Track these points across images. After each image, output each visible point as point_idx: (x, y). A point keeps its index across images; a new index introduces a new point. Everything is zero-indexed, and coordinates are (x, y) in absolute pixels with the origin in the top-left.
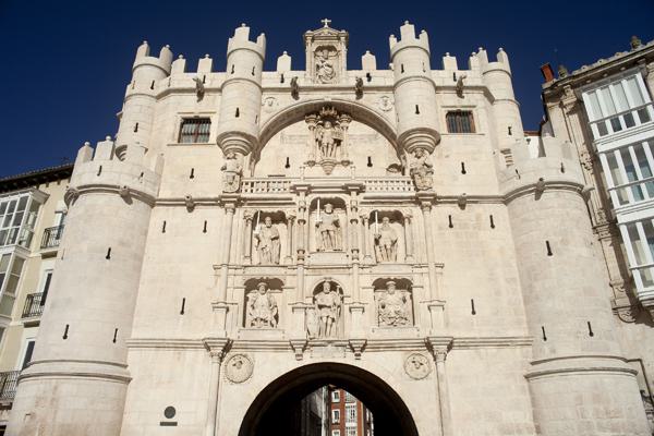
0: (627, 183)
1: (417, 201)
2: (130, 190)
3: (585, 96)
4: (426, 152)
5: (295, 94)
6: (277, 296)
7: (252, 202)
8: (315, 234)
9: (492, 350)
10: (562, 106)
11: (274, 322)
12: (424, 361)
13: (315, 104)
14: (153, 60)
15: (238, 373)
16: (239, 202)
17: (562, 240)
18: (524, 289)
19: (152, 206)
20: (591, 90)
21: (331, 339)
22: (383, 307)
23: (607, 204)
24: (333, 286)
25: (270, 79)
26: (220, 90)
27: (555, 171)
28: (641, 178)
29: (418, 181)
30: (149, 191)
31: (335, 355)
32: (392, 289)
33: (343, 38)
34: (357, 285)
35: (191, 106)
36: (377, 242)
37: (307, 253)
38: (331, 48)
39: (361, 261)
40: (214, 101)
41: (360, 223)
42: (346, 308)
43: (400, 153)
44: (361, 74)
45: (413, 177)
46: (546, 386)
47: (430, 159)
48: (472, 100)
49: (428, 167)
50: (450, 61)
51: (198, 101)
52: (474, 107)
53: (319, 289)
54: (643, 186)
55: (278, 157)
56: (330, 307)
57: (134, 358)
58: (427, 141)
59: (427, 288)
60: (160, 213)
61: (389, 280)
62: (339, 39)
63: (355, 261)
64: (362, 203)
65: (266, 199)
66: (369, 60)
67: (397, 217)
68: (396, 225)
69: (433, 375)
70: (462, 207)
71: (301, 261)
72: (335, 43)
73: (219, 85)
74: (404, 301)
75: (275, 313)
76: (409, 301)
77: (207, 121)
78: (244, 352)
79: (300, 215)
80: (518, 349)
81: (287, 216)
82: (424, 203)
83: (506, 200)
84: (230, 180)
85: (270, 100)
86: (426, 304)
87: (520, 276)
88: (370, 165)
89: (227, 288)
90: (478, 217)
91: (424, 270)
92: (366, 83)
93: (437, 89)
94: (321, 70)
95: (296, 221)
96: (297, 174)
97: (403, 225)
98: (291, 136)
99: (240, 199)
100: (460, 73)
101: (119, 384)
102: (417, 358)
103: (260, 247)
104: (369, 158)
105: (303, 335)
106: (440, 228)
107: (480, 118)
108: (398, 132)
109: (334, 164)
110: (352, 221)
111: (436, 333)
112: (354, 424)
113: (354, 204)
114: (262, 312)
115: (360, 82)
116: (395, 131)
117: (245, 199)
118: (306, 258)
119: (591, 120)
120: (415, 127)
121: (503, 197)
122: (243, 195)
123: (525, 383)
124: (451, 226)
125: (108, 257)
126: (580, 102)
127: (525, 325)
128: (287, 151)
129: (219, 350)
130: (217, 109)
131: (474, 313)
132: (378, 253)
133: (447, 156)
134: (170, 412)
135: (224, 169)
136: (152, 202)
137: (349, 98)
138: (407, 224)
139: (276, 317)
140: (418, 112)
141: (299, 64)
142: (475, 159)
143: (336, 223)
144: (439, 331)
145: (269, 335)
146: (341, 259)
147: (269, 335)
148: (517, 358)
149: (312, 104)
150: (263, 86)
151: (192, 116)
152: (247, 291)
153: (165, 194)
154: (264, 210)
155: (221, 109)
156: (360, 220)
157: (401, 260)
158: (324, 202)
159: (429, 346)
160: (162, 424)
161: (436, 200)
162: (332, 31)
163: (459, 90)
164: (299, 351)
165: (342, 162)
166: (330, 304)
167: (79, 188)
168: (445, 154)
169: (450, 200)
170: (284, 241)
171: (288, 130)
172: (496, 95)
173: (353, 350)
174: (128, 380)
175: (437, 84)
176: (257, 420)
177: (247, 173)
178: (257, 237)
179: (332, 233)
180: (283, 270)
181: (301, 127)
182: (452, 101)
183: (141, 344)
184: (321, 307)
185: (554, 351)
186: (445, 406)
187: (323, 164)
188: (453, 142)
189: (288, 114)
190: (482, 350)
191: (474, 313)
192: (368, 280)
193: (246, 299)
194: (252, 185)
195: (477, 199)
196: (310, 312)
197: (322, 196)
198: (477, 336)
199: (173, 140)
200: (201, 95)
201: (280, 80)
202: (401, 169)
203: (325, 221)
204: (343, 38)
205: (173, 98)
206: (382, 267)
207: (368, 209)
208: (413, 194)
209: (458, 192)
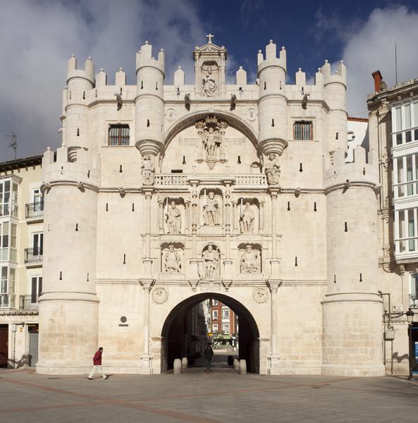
0: (406, 182)
1: (268, 191)
2: (84, 184)
3: (394, 110)
5: (188, 107)
6: (180, 252)
7: (163, 191)
8: (202, 213)
9: (305, 288)
10: (378, 115)
11: (179, 269)
12: (264, 292)
13: (202, 114)
14: (80, 73)
16: (154, 191)
18: (328, 252)
19: (98, 192)
20: (398, 106)
23: (391, 194)
24: (214, 247)
25: (169, 93)
26: (134, 102)
28: (414, 179)
29: (270, 178)
30: (95, 184)
33: (222, 54)
34: (229, 247)
35: (112, 114)
36: (241, 219)
37: (198, 227)
38: (213, 63)
39: (231, 232)
42: (222, 261)
43: (259, 154)
45: (267, 174)
46: (331, 308)
47: (279, 160)
48: (313, 111)
49: (278, 168)
50: (300, 76)
51: (118, 110)
53: (206, 248)
54: (415, 184)
57: (99, 289)
58: (278, 148)
59: (270, 250)
60: (103, 198)
61: (248, 244)
62: (220, 55)
63: (228, 232)
64: (233, 192)
66: (241, 74)
67: (255, 202)
68: (254, 207)
70: (297, 196)
72: (216, 58)
74: (256, 257)
76: (259, 257)
77: (127, 126)
78: (161, 286)
79: (193, 201)
80: (319, 287)
81: (185, 201)
82: (273, 193)
83: (326, 192)
84: (148, 176)
85: (171, 111)
86: (269, 260)
87: (327, 243)
88: (239, 162)
90: (307, 204)
93: (288, 102)
94: (207, 84)
95: (191, 204)
96: (190, 171)
97: (259, 208)
99: (154, 189)
100: (307, 89)
101: (95, 304)
103: (169, 221)
105: (198, 278)
106: (282, 211)
107: (318, 128)
108: (260, 140)
111: (272, 277)
112: (228, 321)
113: (228, 193)
114: (171, 263)
116: (257, 138)
117: (158, 189)
118: (198, 230)
119: (393, 132)
120: (270, 137)
121: (324, 190)
122: (156, 186)
123: (321, 306)
124: (289, 209)
126: (390, 113)
127: (326, 274)
129: (148, 286)
131: (296, 265)
132: (242, 224)
134: (124, 319)
135: (143, 167)
136: (97, 190)
137: (225, 110)
139: (180, 267)
141: (189, 80)
143: (216, 206)
144: (275, 277)
146: (218, 231)
147: (176, 277)
148: (319, 292)
149: (200, 115)
150: (165, 99)
151: (116, 123)
152: (162, 250)
153: (104, 184)
154: (170, 197)
155: (136, 119)
156: (231, 204)
157: (256, 231)
158: (209, 191)
159: (268, 284)
160: (120, 325)
161: (280, 191)
162: (215, 47)
163: (304, 104)
164: (194, 286)
165: (221, 160)
167: (51, 183)
168: (290, 156)
169: (289, 191)
170: (183, 218)
171: (183, 134)
172: (330, 105)
174: (98, 302)
175: (289, 99)
176: (170, 324)
177: (157, 171)
178: (167, 215)
179: (214, 213)
181: (192, 131)
182: (298, 113)
183: (102, 282)
184: (206, 261)
185: (339, 289)
186: (274, 318)
188: (296, 146)
189: (184, 122)
190: (298, 287)
191: (296, 265)
192: (235, 244)
193: (162, 254)
194: (162, 178)
195: (307, 191)
196: (200, 264)
197: (208, 187)
198: (297, 279)
199: (105, 142)
200: (120, 106)
202: (260, 166)
203: (209, 204)
204: (222, 54)
205: (101, 107)
208: (266, 186)
209: (296, 186)
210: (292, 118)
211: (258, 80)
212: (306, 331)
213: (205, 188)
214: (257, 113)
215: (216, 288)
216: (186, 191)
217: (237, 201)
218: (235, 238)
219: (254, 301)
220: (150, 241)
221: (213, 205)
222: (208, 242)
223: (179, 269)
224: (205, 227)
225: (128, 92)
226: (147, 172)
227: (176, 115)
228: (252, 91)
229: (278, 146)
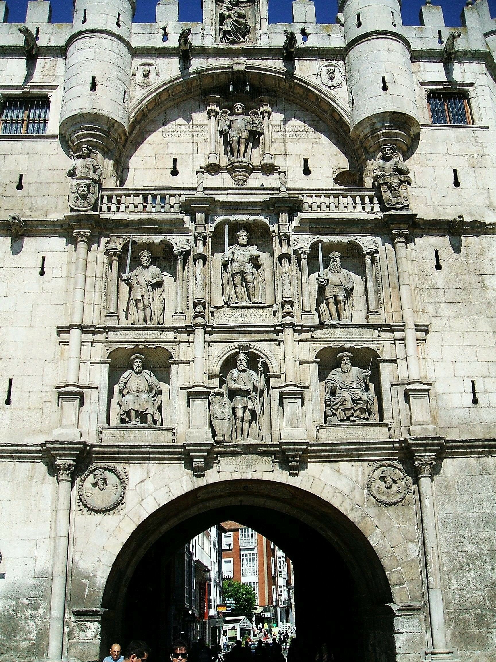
22: (333, 393)
31: (258, 467)
32: (346, 365)
39: (296, 320)
40: (54, 67)
42: (275, 393)
45: (377, 189)
52: (471, 84)
56: (247, 393)
61: (343, 349)
71: (199, 320)
73: (59, 41)
75: (157, 404)
78: (111, 464)
85: (147, 68)
92: (299, 42)
104: (306, 161)
109: (250, 170)
110: (281, 257)
113: (284, 229)
115: (291, 38)
118: (207, 313)
128: (174, 149)
130: (59, 82)
138: (368, 262)
139: (160, 409)
143: (255, 262)
154: (139, 240)
157: (359, 318)
158: (236, 227)
164: (198, 463)
166: (248, 387)
176: (130, 572)
179: (249, 277)
180: (170, 336)
184: (233, 393)
187: (231, 170)
191: (475, 401)
197: (232, 218)
211: (340, 16)
213: (228, 221)
214: (343, 71)
218: (308, 336)
223: (157, 416)
224: (226, 311)
226: (82, 181)
227: (158, 75)
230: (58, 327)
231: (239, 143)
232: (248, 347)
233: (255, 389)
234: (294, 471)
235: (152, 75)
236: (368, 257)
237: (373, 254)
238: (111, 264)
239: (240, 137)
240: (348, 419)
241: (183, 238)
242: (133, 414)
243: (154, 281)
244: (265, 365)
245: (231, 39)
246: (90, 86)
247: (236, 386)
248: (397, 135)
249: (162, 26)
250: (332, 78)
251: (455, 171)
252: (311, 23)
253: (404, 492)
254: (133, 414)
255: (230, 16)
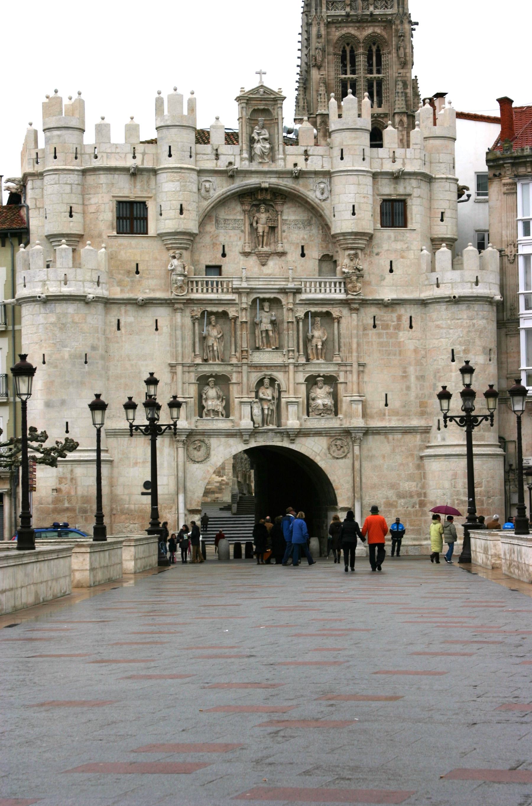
4: (359, 252)
9: (398, 436)
13: (251, 188)
15: (199, 455)
17: (464, 350)
21: (271, 427)
24: (273, 381)
27: (469, 285)
31: (275, 439)
37: (250, 352)
41: (295, 323)
44: (300, 149)
49: (359, 270)
52: (410, 195)
53: (260, 383)
55: (214, 244)
56: (270, 401)
60: (115, 314)
61: (319, 376)
65: (211, 300)
69: (350, 455)
71: (245, 361)
79: (244, 317)
80: (418, 436)
85: (207, 185)
88: (303, 255)
89: (184, 383)
91: (349, 368)
95: (238, 323)
98: (225, 220)
102: (339, 442)
104: (303, 247)
105: (250, 425)
106: (365, 329)
109: (269, 255)
113: (291, 306)
124: (375, 326)
125: (86, 362)
131: (386, 405)
133: (377, 254)
137: (286, 183)
140: (354, 214)
142: (402, 257)
145: (222, 424)
147: (222, 424)
149: (247, 189)
154: (209, 309)
156: (294, 320)
158: (263, 300)
164: (246, 437)
166: (270, 398)
173: (288, 436)
179: (271, 333)
180: (229, 368)
184: (261, 400)
185: (444, 439)
187: (259, 255)
190: (390, 437)
191: (386, 405)
192: (301, 378)
197: (261, 296)
199: (113, 229)
201: (214, 157)
203: (265, 320)
206: (313, 366)
207: (302, 309)
210: (378, 195)
212: (400, 496)
213: (258, 298)
215: (277, 439)
216: (230, 303)
217: (302, 315)
218: (301, 369)
219: (330, 457)
220: (183, 372)
221: (269, 321)
222: (263, 373)
225: (144, 154)
227: (215, 190)
228: (322, 156)
229: (360, 242)
230: (170, 364)
231: (263, 236)
232: (270, 375)
233: (273, 398)
234: (292, 441)
235: (212, 191)
236: (336, 321)
237: (339, 319)
238: (194, 324)
239: (263, 232)
240: (320, 414)
241: (234, 309)
242: (211, 412)
243: (219, 336)
244: (279, 385)
245: (260, 160)
246: (179, 211)
247: (264, 397)
248: (358, 243)
249: (215, 148)
250: (322, 194)
251: (391, 262)
252: (311, 146)
253: (346, 451)
254: (211, 412)
255: (258, 141)
